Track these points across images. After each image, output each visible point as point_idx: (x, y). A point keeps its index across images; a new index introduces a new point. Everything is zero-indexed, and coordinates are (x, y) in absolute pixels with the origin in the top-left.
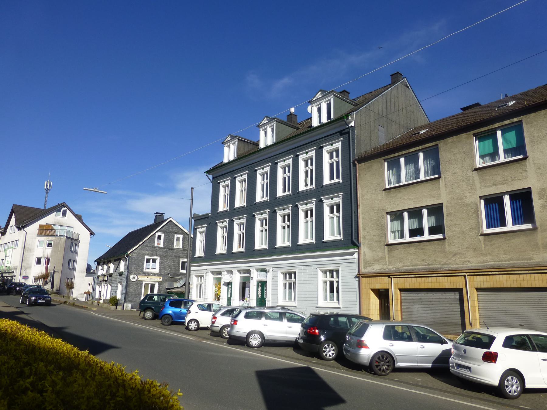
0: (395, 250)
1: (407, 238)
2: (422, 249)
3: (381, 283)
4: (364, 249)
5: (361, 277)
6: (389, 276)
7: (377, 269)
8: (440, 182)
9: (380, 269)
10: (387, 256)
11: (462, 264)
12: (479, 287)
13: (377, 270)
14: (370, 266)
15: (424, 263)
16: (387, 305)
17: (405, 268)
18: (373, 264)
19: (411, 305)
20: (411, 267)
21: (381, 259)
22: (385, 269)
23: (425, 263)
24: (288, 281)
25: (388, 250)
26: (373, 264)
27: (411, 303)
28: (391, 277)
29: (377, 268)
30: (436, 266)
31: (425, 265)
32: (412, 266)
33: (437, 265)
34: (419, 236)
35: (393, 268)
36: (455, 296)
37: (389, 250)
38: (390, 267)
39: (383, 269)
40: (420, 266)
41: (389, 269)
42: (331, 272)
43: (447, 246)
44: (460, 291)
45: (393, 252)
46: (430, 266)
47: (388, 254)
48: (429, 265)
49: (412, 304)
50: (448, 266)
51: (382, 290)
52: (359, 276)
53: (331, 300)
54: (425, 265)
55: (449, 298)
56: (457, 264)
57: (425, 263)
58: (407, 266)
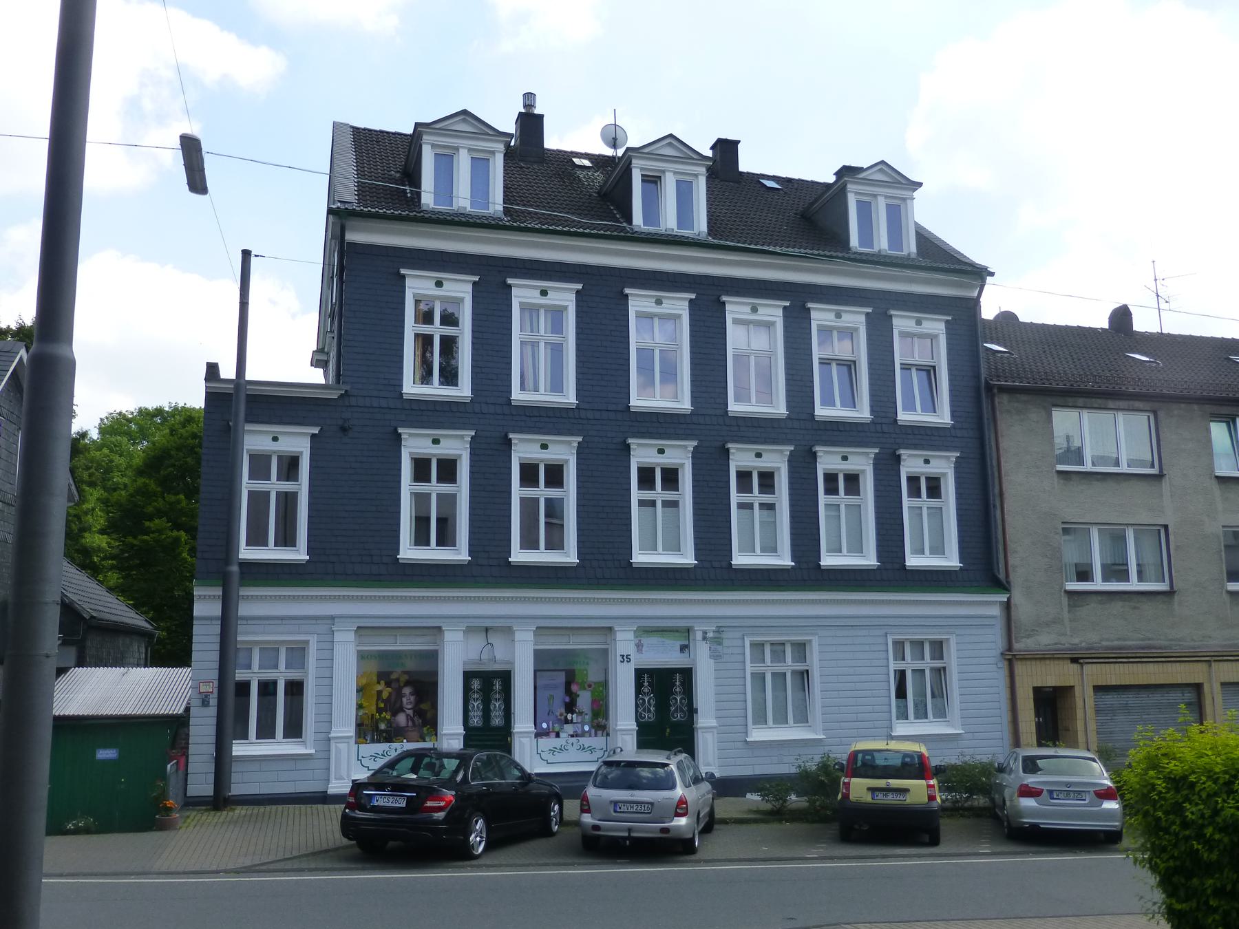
0: (1082, 606)
1: (1098, 584)
2: (1135, 608)
3: (1053, 675)
4: (1018, 596)
5: (1014, 660)
6: (1074, 660)
7: (1047, 643)
8: (1162, 484)
9: (1053, 644)
10: (1066, 615)
11: (1201, 641)
12: (1227, 680)
13: (1046, 645)
14: (1029, 636)
15: (1139, 635)
16: (1039, 719)
17: (1105, 643)
18: (1037, 631)
19: (1109, 718)
20: (1116, 643)
21: (1055, 623)
22: (1064, 645)
23: (1142, 636)
24: (769, 667)
25: (1069, 605)
26: (1037, 631)
27: (1109, 715)
28: (1081, 661)
29: (1045, 640)
30: (1162, 642)
31: (1143, 640)
32: (1119, 639)
33: (1161, 640)
34: (1114, 580)
35: (1081, 644)
36: (1184, 698)
37: (1071, 603)
38: (1076, 641)
39: (1061, 644)
40: (1133, 640)
41: (1075, 645)
42: (918, 645)
43: (1176, 606)
44: (1198, 687)
45: (1081, 608)
46: (1150, 642)
47: (1069, 612)
48: (1149, 639)
49: (1112, 715)
50: (1181, 643)
51: (1048, 689)
52: (1011, 658)
53: (916, 717)
54: (1143, 640)
55: (1173, 701)
56: (1193, 640)
57: (1142, 636)
58: (1108, 640)
